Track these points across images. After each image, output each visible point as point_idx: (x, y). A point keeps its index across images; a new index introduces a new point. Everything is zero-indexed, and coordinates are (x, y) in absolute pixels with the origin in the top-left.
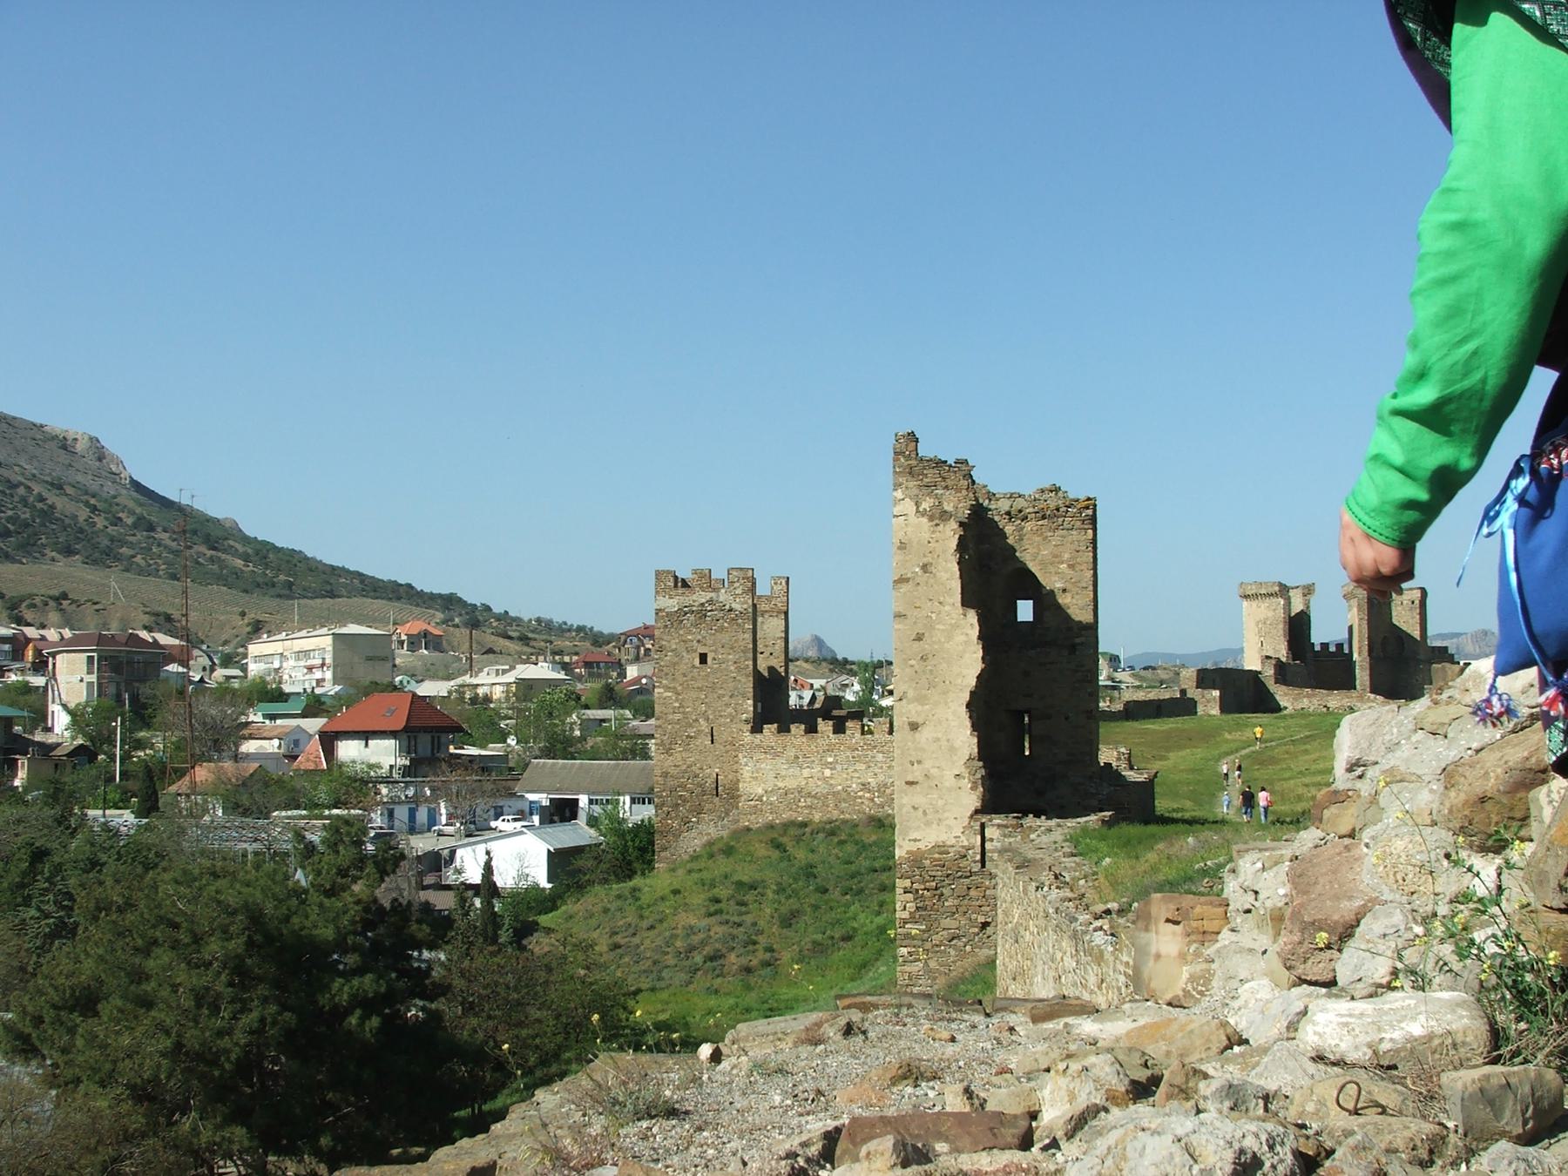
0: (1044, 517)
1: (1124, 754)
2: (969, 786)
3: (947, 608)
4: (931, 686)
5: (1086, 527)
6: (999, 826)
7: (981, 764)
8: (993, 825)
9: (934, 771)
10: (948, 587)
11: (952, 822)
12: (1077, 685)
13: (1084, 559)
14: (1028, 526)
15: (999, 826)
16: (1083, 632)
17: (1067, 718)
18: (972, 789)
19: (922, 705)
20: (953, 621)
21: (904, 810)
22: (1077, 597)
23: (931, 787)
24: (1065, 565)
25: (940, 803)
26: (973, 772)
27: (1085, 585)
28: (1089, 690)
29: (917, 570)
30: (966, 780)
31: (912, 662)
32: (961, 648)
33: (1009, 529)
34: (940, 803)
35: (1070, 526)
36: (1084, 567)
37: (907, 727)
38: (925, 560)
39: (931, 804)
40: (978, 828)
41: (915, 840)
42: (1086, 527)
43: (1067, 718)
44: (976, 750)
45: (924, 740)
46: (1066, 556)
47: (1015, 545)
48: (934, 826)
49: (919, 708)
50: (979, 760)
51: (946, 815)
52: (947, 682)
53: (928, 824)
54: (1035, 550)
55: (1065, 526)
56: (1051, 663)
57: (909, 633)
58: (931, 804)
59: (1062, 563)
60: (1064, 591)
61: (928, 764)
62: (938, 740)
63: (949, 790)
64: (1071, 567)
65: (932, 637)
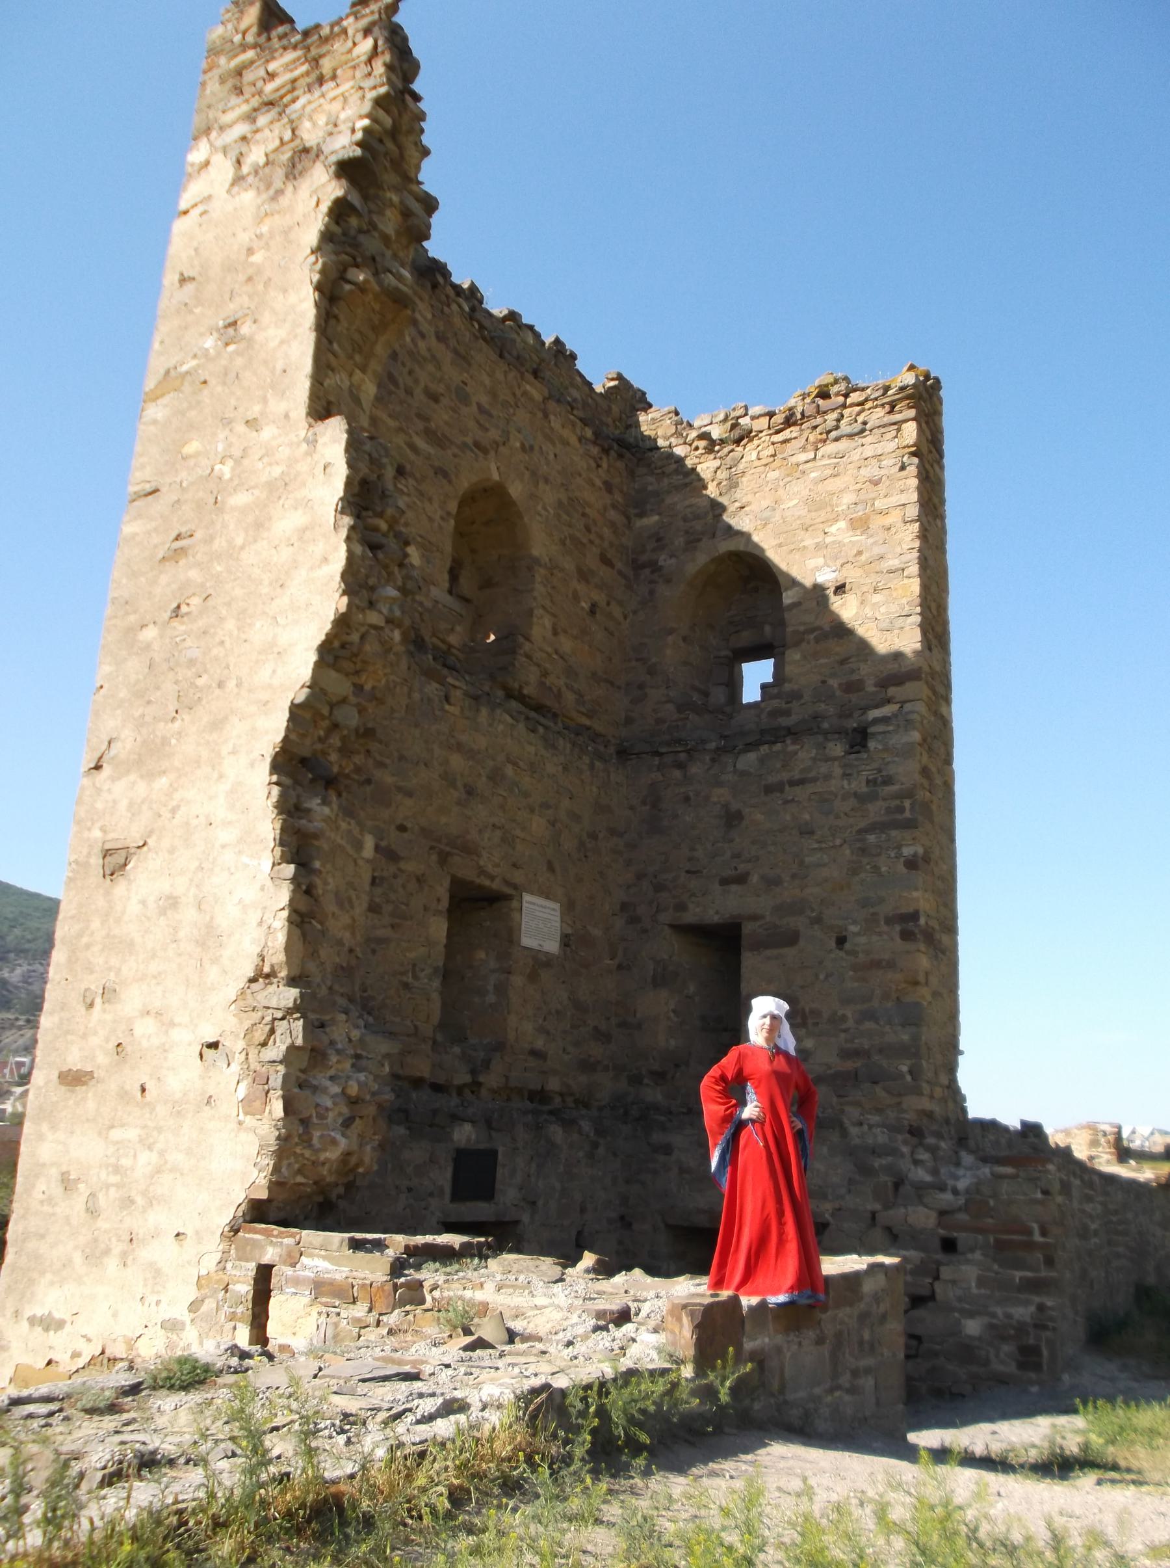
0: (789, 422)
1: (1105, 1134)
2: (242, 1090)
3: (268, 433)
4: (186, 703)
5: (897, 417)
6: (321, 1288)
7: (291, 995)
8: (297, 1282)
9: (145, 1029)
10: (279, 366)
11: (163, 1252)
12: (872, 838)
13: (897, 499)
14: (750, 452)
15: (321, 1288)
16: (892, 691)
17: (841, 941)
18: (247, 1105)
19: (151, 776)
20: (277, 471)
21: (41, 1186)
22: (877, 598)
23: (123, 1095)
24: (842, 524)
25: (146, 1159)
26: (260, 1034)
27: (894, 563)
28: (907, 851)
29: (209, 343)
30: (235, 1067)
31: (150, 633)
32: (286, 553)
33: (706, 467)
34: (146, 1159)
35: (857, 427)
36: (894, 518)
37: (96, 861)
38: (231, 309)
39: (117, 1169)
40: (244, 1288)
41: (50, 1324)
42: (897, 417)
43: (841, 941)
44: (281, 938)
45: (134, 908)
46: (848, 499)
47: (720, 499)
48: (112, 1264)
49: (141, 789)
50: (292, 982)
51: (157, 1218)
52: (231, 684)
53: (95, 1254)
54: (765, 504)
55: (845, 428)
56: (801, 782)
57: (156, 539)
58: (117, 1169)
59: (836, 520)
60: (840, 589)
61: (132, 1000)
62: (172, 903)
63: (178, 1110)
64: (859, 524)
65: (209, 540)
